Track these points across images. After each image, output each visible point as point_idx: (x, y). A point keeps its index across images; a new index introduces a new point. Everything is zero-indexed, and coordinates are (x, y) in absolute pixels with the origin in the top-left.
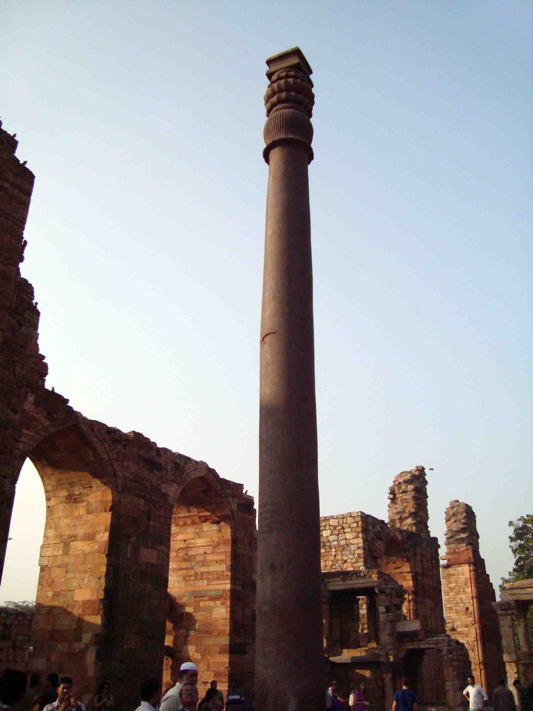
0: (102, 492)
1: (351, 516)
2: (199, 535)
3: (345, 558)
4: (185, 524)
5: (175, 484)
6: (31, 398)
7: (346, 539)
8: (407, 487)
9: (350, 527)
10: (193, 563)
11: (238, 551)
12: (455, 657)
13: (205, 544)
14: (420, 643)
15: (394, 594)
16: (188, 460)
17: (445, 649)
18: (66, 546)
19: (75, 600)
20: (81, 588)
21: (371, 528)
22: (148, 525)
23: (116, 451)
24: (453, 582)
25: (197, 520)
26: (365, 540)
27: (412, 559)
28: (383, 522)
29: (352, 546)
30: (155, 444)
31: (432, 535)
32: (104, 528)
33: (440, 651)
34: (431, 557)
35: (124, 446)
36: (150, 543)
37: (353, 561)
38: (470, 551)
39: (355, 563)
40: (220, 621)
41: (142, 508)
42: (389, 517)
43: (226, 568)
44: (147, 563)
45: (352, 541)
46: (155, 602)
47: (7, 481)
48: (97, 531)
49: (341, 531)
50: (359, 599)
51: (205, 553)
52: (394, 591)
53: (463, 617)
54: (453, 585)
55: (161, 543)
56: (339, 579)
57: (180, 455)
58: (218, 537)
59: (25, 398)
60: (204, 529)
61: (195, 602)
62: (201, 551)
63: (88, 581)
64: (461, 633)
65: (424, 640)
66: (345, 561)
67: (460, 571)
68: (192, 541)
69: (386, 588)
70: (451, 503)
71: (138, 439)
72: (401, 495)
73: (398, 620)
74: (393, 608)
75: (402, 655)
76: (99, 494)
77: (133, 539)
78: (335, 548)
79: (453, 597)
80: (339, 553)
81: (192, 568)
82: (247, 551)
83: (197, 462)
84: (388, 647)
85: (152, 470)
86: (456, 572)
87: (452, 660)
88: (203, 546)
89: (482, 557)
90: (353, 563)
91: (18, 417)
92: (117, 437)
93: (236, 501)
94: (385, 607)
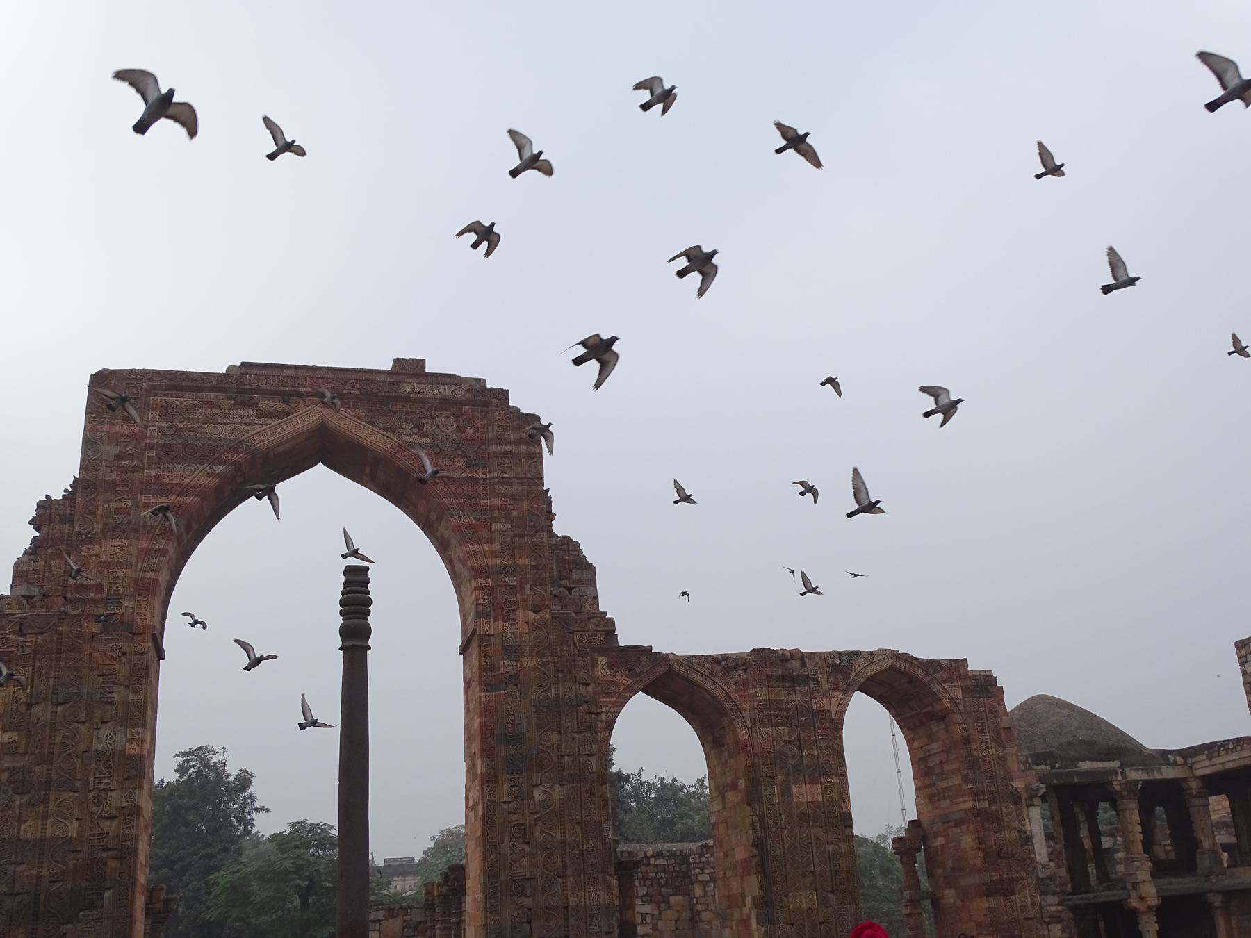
2: (931, 738)
6: (603, 662)
16: (854, 655)
23: (733, 681)
35: (745, 670)
47: (594, 760)
55: (826, 773)
56: (1204, 757)
57: (840, 653)
59: (594, 665)
60: (934, 729)
62: (937, 760)
71: (763, 656)
77: (779, 778)
83: (871, 653)
91: (590, 688)
93: (958, 684)
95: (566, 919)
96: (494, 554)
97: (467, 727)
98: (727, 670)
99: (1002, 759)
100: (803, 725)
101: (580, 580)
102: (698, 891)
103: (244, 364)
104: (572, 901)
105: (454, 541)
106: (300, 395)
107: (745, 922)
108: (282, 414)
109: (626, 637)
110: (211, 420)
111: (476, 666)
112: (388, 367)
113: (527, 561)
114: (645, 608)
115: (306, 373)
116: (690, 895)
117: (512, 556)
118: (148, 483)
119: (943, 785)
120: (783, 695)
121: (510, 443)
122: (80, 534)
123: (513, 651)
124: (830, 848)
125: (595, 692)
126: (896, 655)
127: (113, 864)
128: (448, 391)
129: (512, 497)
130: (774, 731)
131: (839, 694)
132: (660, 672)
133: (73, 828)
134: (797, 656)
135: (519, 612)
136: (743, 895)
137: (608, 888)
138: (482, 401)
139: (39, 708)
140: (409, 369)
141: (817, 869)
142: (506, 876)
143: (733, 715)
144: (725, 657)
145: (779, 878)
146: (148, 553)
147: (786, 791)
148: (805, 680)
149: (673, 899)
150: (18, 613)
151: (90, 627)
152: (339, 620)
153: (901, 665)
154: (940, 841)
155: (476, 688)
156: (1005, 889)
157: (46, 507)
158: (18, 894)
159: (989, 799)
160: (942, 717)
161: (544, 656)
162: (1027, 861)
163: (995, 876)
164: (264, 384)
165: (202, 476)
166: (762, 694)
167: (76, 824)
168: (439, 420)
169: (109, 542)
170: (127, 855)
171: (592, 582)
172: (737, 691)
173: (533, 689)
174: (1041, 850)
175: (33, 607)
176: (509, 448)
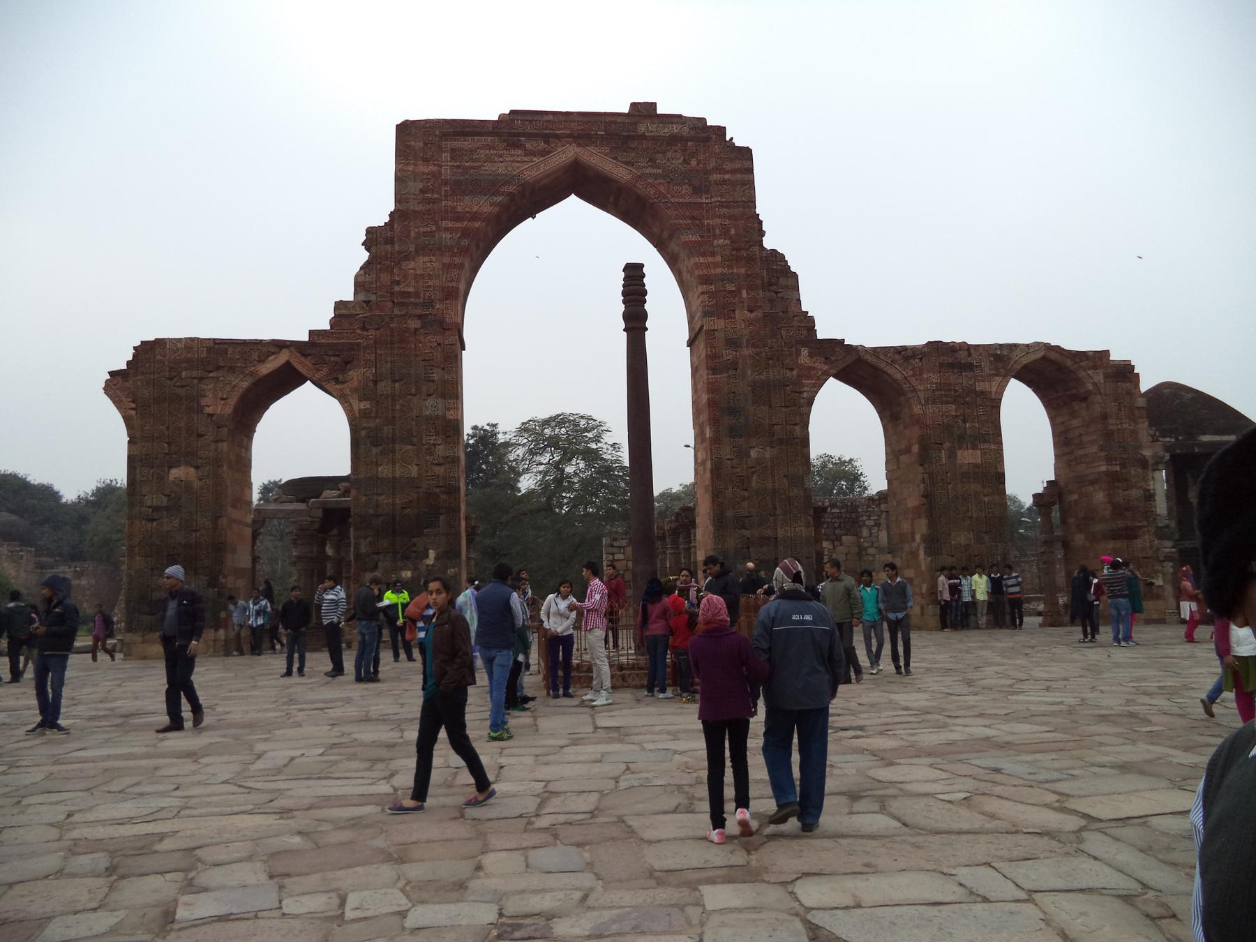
2: (1073, 415)
6: (805, 352)
16: (1015, 345)
18: (898, 460)
47: (797, 428)
55: (985, 441)
59: (798, 354)
62: (1077, 433)
71: (936, 347)
77: (947, 445)
83: (1028, 346)
91: (795, 372)
92: (910, 353)
95: (776, 547)
96: (716, 265)
97: (695, 403)
98: (906, 359)
99: (1134, 433)
101: (786, 286)
102: (865, 532)
103: (512, 112)
104: (781, 533)
105: (682, 256)
106: (557, 137)
107: (914, 554)
108: (544, 153)
109: (823, 333)
110: (489, 159)
111: (703, 354)
112: (626, 110)
113: (743, 271)
114: (840, 308)
115: (562, 118)
116: (858, 535)
117: (730, 267)
118: (446, 212)
119: (1081, 452)
120: (952, 378)
121: (727, 172)
122: (399, 252)
123: (733, 343)
124: (986, 499)
125: (798, 376)
126: (1047, 347)
127: (443, 497)
128: (675, 129)
129: (730, 218)
130: (944, 407)
131: (999, 379)
132: (850, 359)
133: (414, 471)
134: (964, 347)
135: (737, 312)
136: (913, 534)
137: (808, 526)
138: (704, 136)
139: (383, 384)
140: (643, 111)
142: (730, 513)
143: (910, 395)
144: (904, 348)
146: (448, 267)
147: (952, 455)
148: (970, 367)
149: (844, 538)
150: (362, 314)
151: (413, 324)
152: (622, 308)
153: (1053, 356)
154: (1075, 497)
155: (703, 373)
156: (1129, 534)
157: (370, 231)
158: (379, 516)
160: (1085, 398)
161: (757, 347)
162: (1149, 514)
163: (1121, 524)
164: (529, 129)
165: (484, 205)
166: (935, 378)
167: (416, 468)
168: (669, 154)
169: (421, 259)
170: (453, 490)
171: (796, 287)
172: (913, 376)
173: (749, 372)
174: (1161, 506)
175: (371, 309)
176: (727, 177)
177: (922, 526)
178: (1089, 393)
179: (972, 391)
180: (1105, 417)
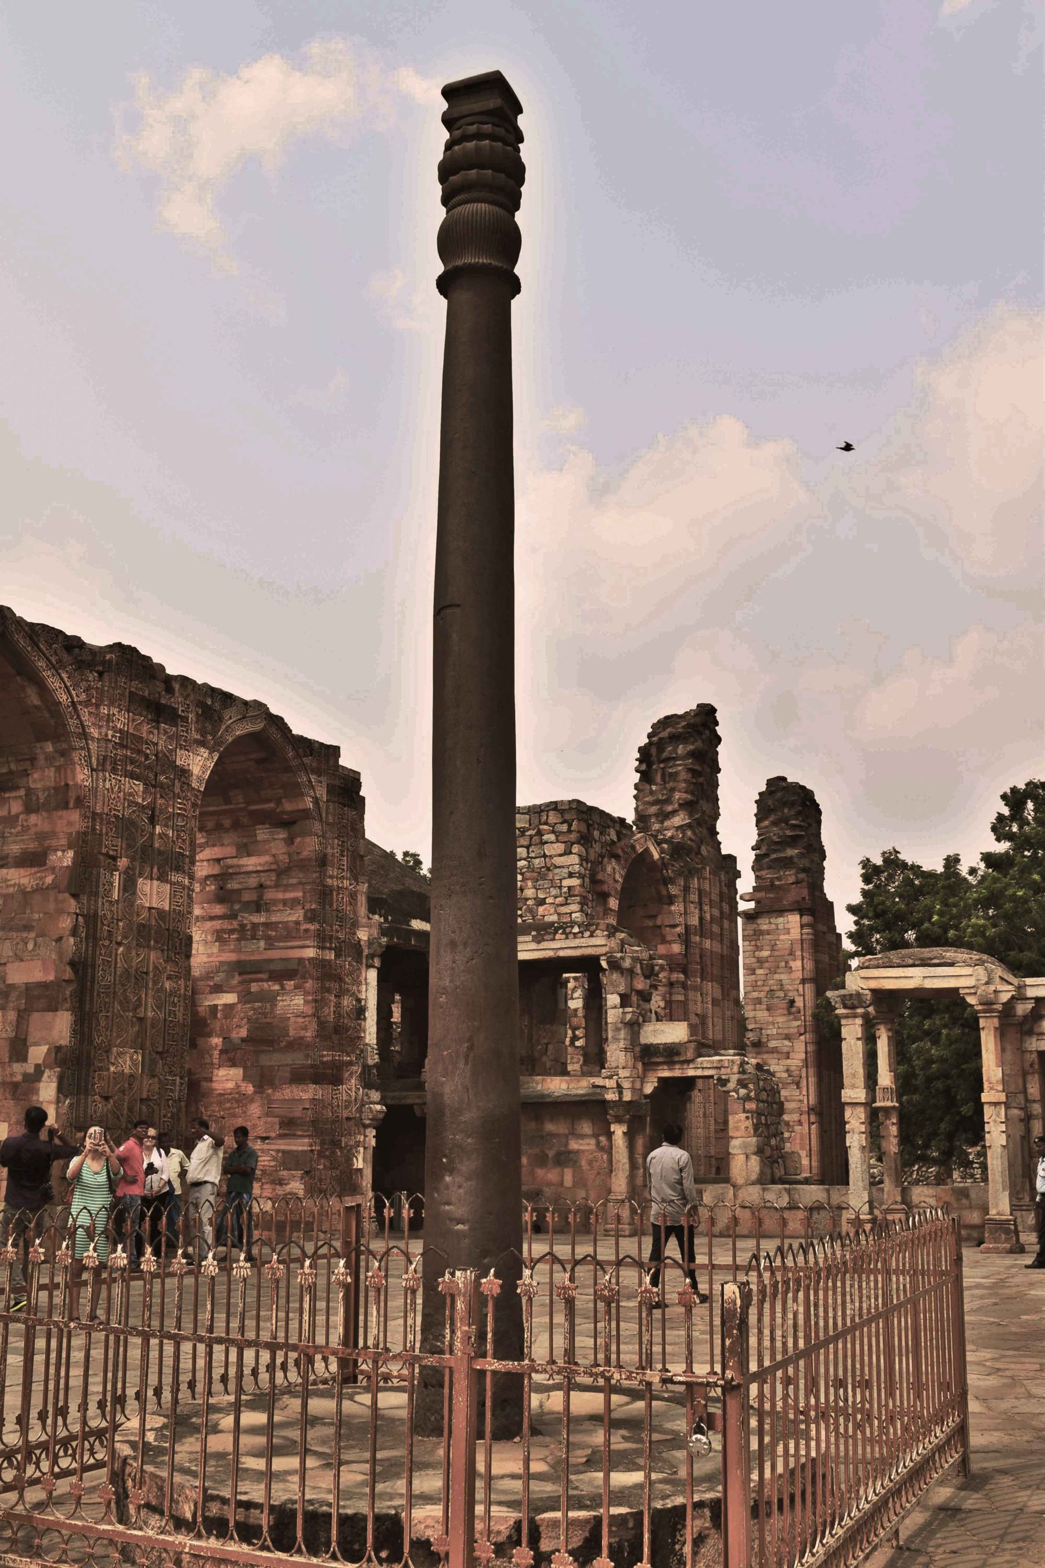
0: (58, 769)
1: (555, 809)
2: (245, 849)
3: (541, 896)
4: (219, 827)
5: (203, 750)
7: (545, 856)
8: (675, 750)
9: (553, 832)
10: (237, 907)
11: (329, 881)
12: (752, 1094)
13: (259, 868)
14: (685, 1066)
15: (639, 971)
17: (734, 1078)
19: (9, 982)
20: (22, 960)
21: (596, 833)
22: (152, 834)
23: (84, 684)
24: (766, 948)
25: (245, 820)
26: (583, 859)
27: (681, 899)
28: (622, 821)
29: (557, 871)
30: (162, 667)
31: (725, 850)
32: (64, 842)
33: (723, 1082)
34: (721, 894)
35: (101, 674)
36: (155, 870)
37: (559, 900)
38: (805, 884)
39: (562, 905)
40: (292, 1020)
41: (140, 801)
42: (636, 809)
43: (305, 916)
44: (150, 908)
45: (558, 861)
46: (168, 985)
48: (49, 847)
49: (536, 839)
50: (567, 980)
51: (261, 886)
52: (639, 966)
53: (781, 1019)
54: (765, 953)
55: (178, 869)
56: (530, 938)
57: (213, 689)
58: (289, 855)
61: (241, 983)
62: (253, 882)
63: (35, 945)
64: (774, 1051)
65: (692, 1061)
66: (542, 902)
67: (781, 927)
68: (235, 861)
69: (622, 958)
70: (770, 782)
72: (662, 765)
73: (644, 1021)
74: (634, 998)
75: (649, 1089)
76: (51, 773)
77: (123, 862)
78: (522, 874)
79: (763, 977)
80: (530, 883)
81: (232, 916)
82: (346, 883)
83: (246, 703)
84: (623, 1073)
85: (158, 722)
86: (773, 926)
87: (747, 1098)
88: (257, 872)
89: (830, 897)
90: (558, 905)
94: (621, 995)
99: (353, 896)
100: (162, 786)
124: (168, 985)
130: (128, 784)
141: (150, 1014)
145: (103, 1023)
147: (129, 886)
153: (275, 734)
154: (230, 998)
156: (330, 1076)
159: (335, 949)
162: (355, 1039)
172: (87, 703)
177: (60, 1026)
178: (305, 814)
179: (166, 762)
180: (323, 861)
